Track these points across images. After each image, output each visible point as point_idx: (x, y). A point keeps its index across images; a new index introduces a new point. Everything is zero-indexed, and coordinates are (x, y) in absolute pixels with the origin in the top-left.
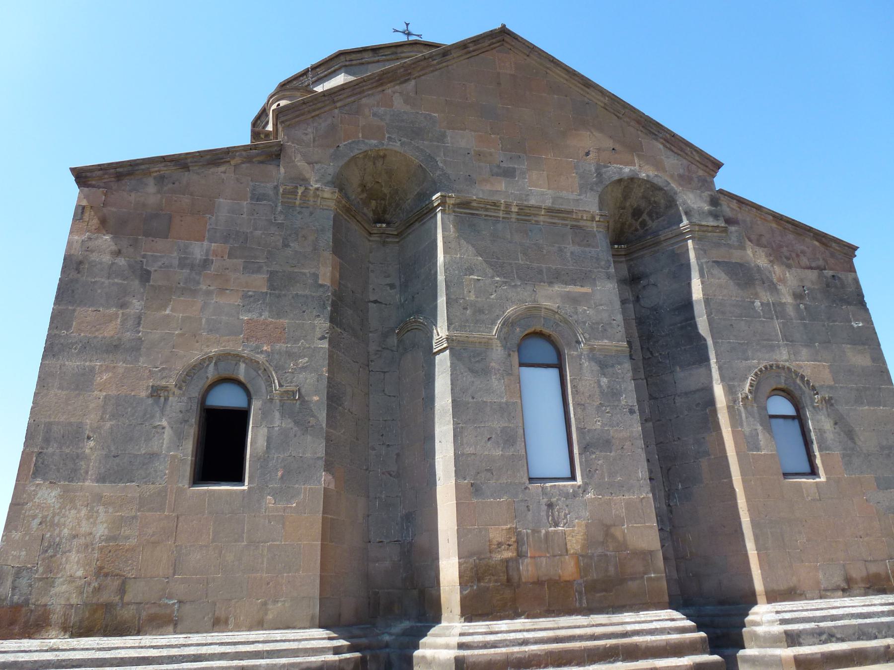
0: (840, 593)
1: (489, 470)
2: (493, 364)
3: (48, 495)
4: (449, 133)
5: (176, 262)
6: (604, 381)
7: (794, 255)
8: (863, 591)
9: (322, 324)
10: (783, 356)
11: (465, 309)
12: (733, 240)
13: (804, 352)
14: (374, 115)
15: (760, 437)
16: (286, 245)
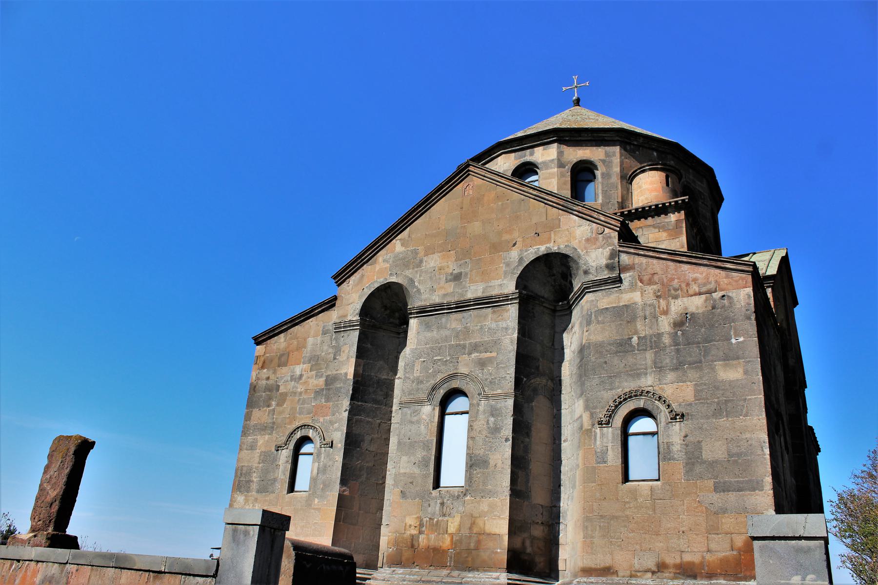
0: (649, 575)
1: (412, 483)
2: (424, 417)
3: (240, 498)
4: (425, 259)
5: (289, 379)
6: (492, 419)
7: (683, 286)
8: (672, 575)
9: (346, 403)
10: (647, 382)
11: (413, 382)
12: (626, 283)
13: (671, 376)
14: (384, 261)
15: (610, 452)
16: (335, 359)
